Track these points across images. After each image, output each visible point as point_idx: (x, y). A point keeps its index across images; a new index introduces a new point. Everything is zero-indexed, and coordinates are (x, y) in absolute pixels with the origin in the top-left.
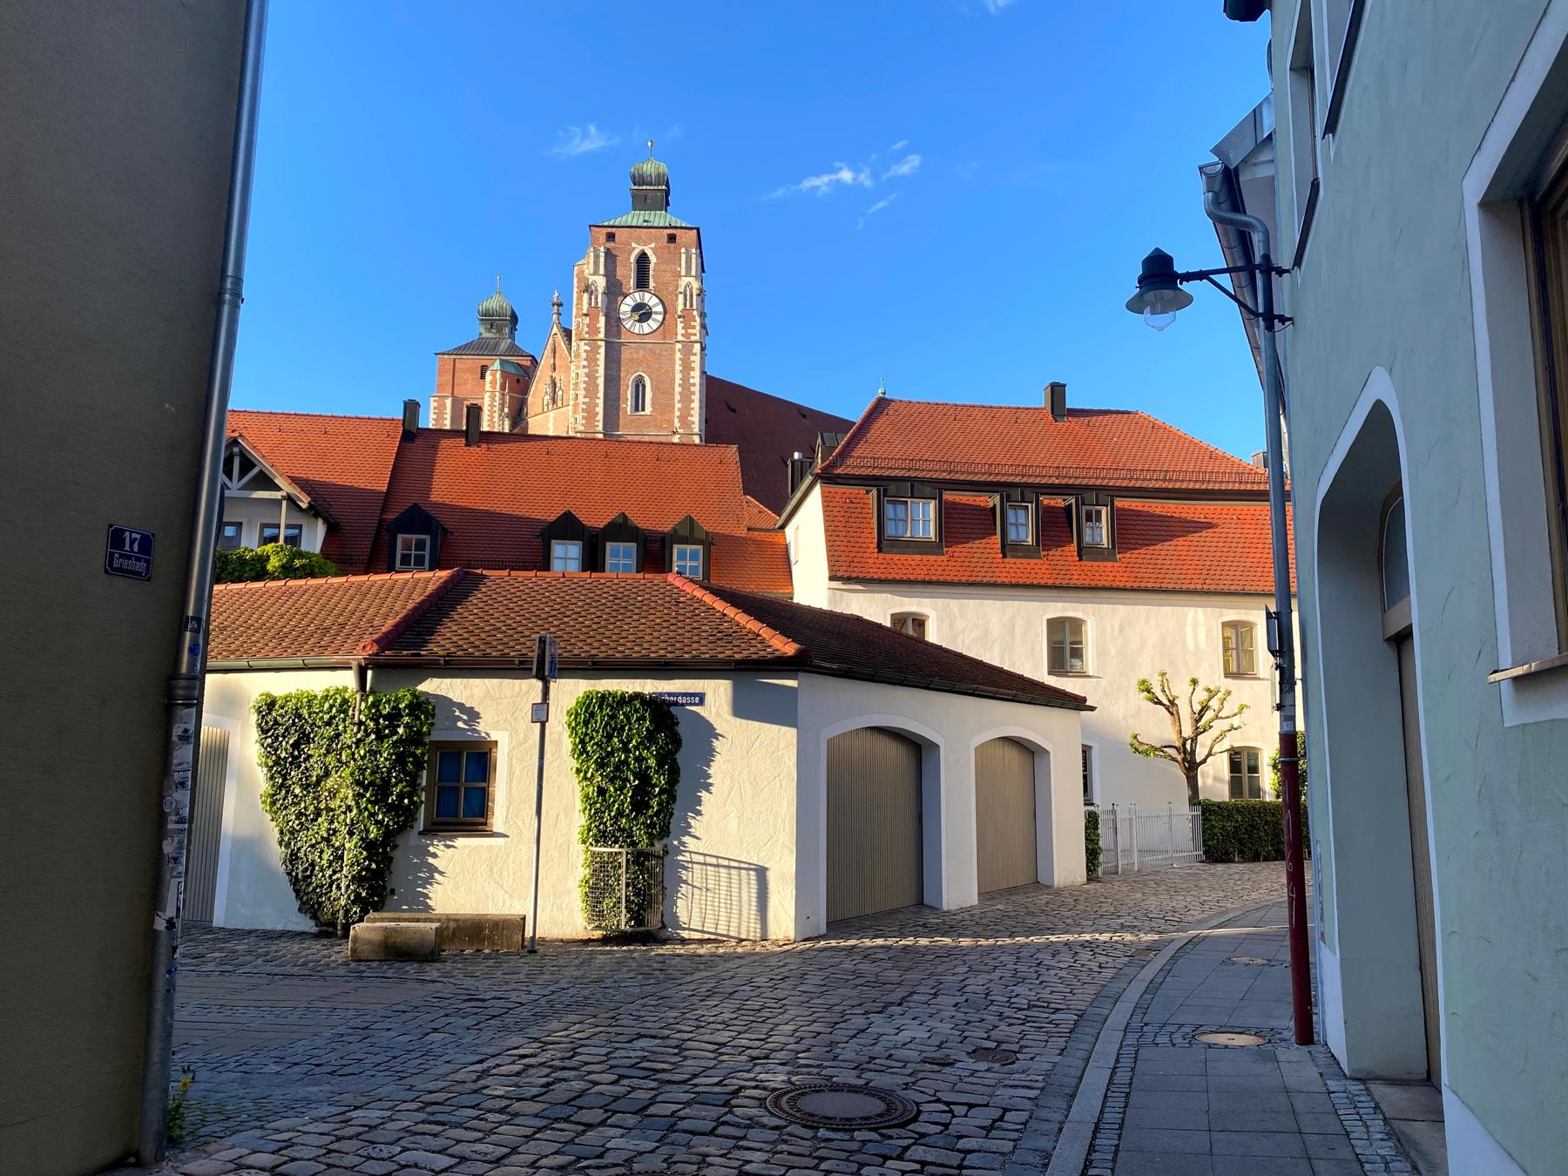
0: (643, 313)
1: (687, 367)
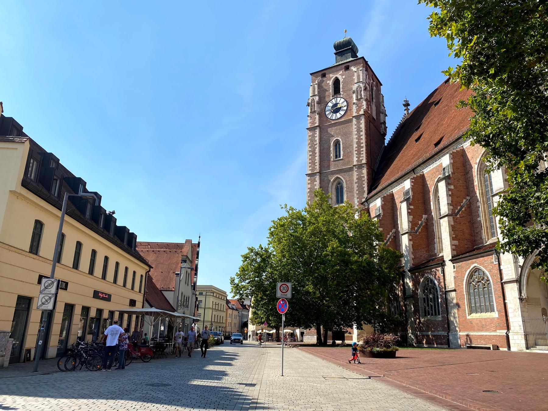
0: (336, 109)
1: (359, 130)
